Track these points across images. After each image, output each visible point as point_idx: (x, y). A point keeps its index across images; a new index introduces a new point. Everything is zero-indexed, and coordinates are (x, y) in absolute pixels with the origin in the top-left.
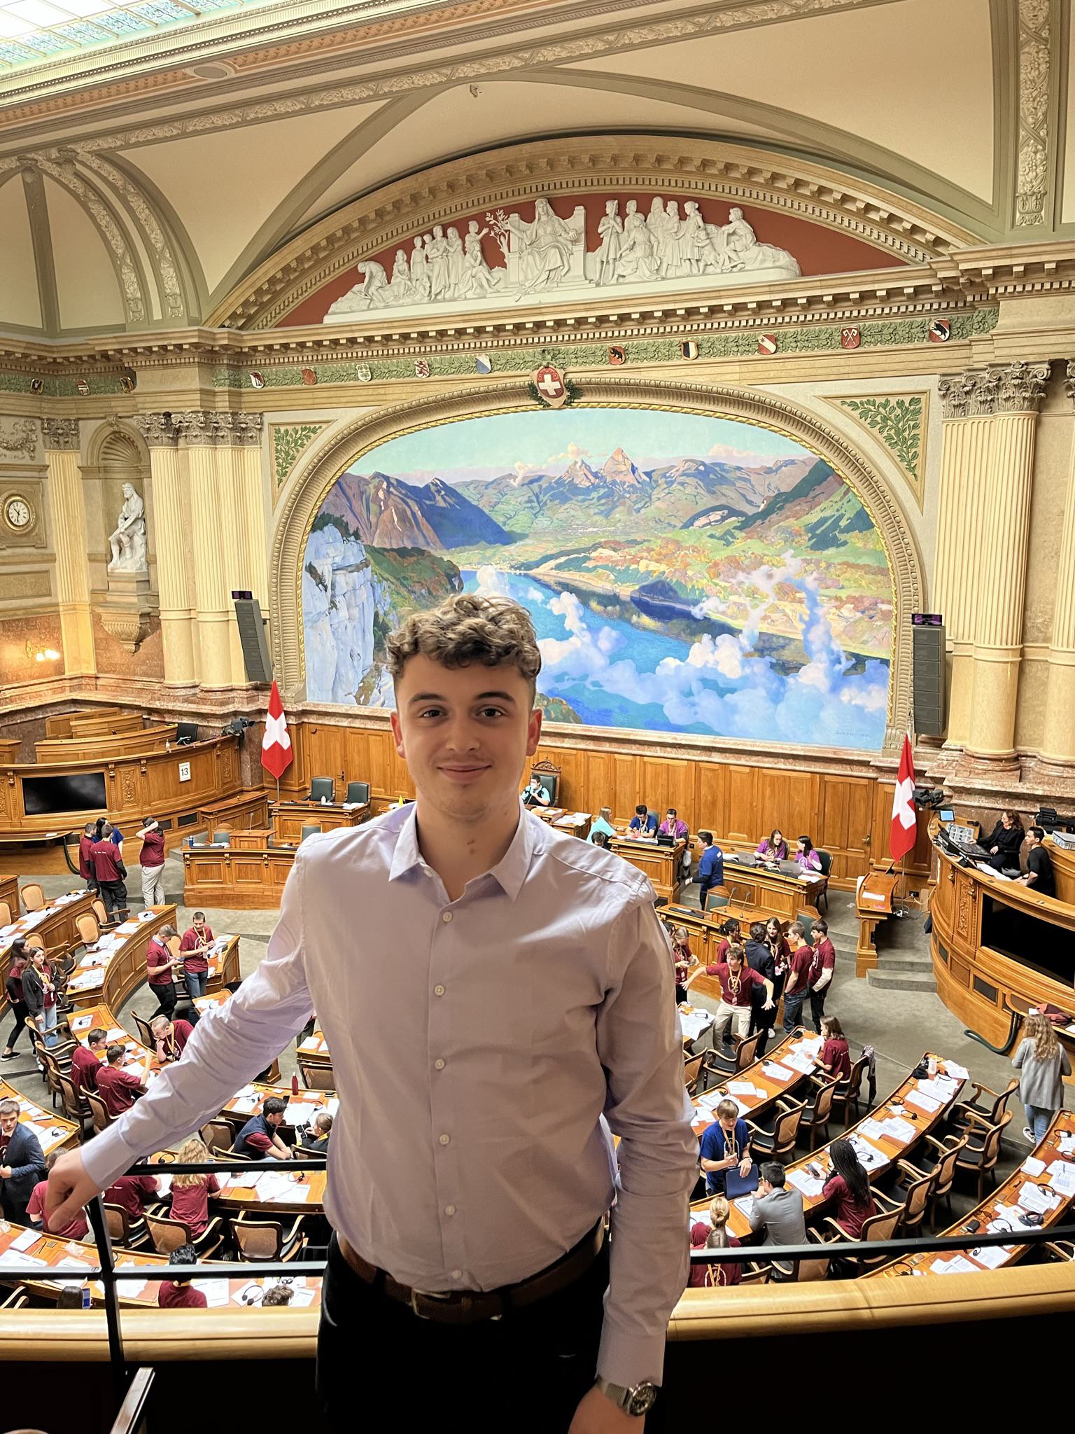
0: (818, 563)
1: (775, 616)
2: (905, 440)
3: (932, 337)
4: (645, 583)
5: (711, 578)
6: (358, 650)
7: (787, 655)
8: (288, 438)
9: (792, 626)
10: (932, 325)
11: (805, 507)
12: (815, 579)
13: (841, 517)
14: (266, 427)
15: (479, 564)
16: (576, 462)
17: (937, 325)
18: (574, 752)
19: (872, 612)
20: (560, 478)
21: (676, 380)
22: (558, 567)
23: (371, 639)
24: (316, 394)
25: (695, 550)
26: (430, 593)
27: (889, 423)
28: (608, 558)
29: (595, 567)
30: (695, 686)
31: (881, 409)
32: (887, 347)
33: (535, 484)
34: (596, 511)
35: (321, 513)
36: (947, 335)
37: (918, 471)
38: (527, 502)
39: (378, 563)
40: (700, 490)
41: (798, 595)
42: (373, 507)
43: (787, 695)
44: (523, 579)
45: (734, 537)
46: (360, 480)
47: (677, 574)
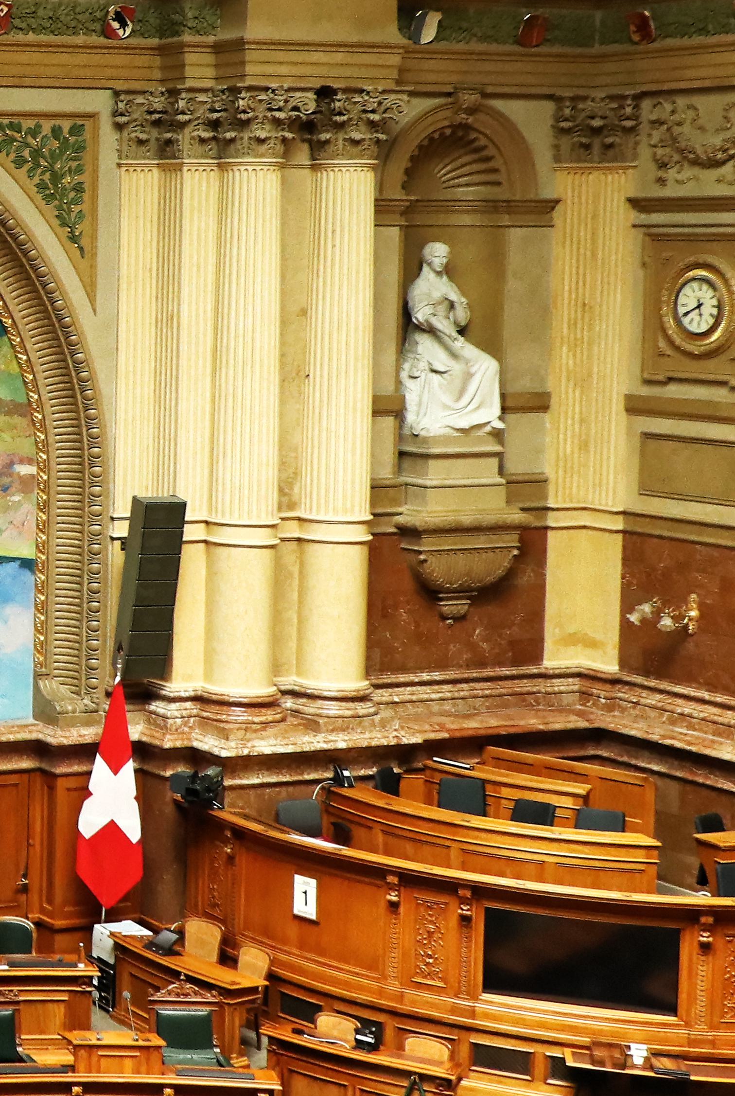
3: (108, 33)
10: (112, 15)
17: (117, 13)
31: (30, 139)
32: (43, 38)
36: (128, 31)
37: (85, 242)
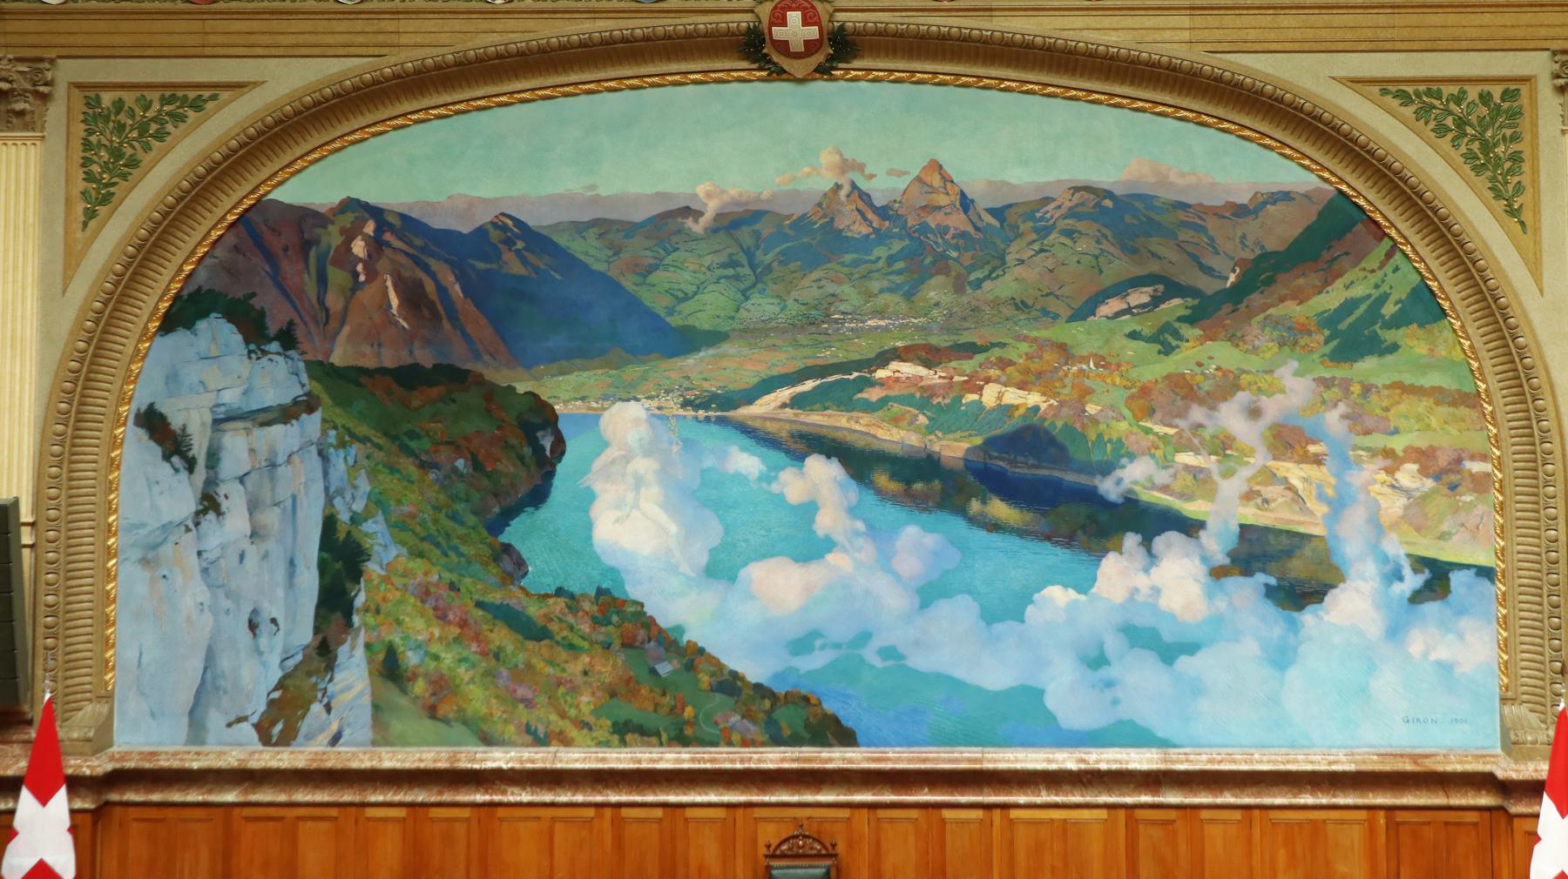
0: (1345, 385)
1: (1270, 491)
2: (1498, 163)
4: (998, 432)
5: (1137, 418)
6: (271, 609)
7: (1297, 568)
8: (122, 117)
9: (1305, 510)
11: (1315, 280)
12: (1344, 417)
13: (1383, 299)
14: (61, 90)
15: (605, 398)
16: (838, 187)
18: (845, 813)
19: (1453, 478)
20: (804, 217)
21: (1065, 35)
22: (797, 402)
23: (309, 581)
24: (210, 25)
25: (1101, 361)
26: (477, 465)
27: (1469, 130)
28: (913, 381)
29: (884, 402)
30: (1113, 644)
31: (1453, 106)
33: (746, 230)
34: (885, 284)
35: (191, 288)
37: (1527, 216)
38: (724, 266)
39: (342, 402)
40: (1106, 246)
41: (1312, 449)
42: (336, 276)
43: (1302, 648)
44: (714, 428)
45: (1180, 338)
46: (305, 219)
47: (1065, 410)
